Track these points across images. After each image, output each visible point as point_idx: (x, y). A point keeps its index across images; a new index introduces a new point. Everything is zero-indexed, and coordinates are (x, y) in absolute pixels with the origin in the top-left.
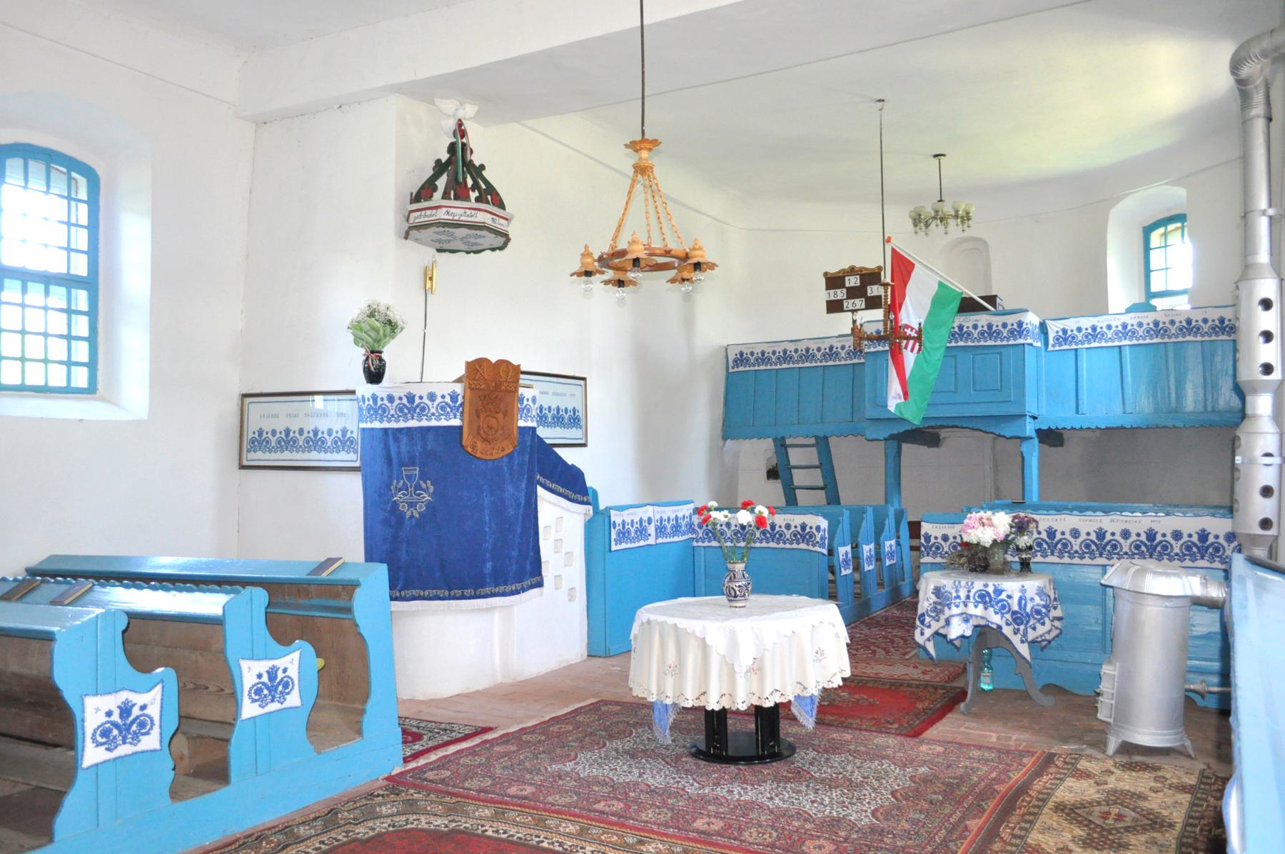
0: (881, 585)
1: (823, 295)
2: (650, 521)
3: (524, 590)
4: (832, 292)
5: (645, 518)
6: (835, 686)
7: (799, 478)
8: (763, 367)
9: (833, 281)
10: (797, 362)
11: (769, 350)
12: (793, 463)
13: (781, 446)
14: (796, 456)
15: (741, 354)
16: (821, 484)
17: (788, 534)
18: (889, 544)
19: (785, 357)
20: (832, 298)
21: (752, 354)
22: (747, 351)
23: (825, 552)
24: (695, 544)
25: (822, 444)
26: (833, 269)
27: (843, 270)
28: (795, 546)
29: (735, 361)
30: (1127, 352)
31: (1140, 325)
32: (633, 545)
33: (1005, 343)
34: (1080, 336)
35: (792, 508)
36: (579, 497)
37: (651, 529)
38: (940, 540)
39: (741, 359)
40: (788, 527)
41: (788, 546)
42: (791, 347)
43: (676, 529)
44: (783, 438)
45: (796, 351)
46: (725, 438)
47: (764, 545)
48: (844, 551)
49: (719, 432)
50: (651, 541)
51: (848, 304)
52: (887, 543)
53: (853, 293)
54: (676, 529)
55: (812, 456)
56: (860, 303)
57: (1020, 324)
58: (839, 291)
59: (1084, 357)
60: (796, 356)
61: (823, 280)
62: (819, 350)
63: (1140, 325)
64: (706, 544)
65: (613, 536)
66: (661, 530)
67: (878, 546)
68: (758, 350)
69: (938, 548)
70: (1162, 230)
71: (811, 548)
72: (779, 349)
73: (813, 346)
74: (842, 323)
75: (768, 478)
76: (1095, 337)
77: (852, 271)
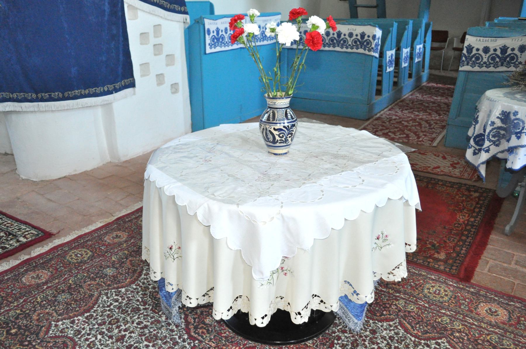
0: (410, 76)
3: (117, 90)
6: (398, 279)
16: (375, 4)
17: (350, 41)
18: (419, 47)
23: (377, 55)
28: (355, 50)
32: (227, 48)
35: (355, 20)
36: (177, 7)
38: (481, 52)
41: (349, 50)
47: (331, 48)
48: (390, 54)
52: (418, 47)
65: (208, 41)
67: (412, 48)
69: (477, 59)
71: (367, 52)
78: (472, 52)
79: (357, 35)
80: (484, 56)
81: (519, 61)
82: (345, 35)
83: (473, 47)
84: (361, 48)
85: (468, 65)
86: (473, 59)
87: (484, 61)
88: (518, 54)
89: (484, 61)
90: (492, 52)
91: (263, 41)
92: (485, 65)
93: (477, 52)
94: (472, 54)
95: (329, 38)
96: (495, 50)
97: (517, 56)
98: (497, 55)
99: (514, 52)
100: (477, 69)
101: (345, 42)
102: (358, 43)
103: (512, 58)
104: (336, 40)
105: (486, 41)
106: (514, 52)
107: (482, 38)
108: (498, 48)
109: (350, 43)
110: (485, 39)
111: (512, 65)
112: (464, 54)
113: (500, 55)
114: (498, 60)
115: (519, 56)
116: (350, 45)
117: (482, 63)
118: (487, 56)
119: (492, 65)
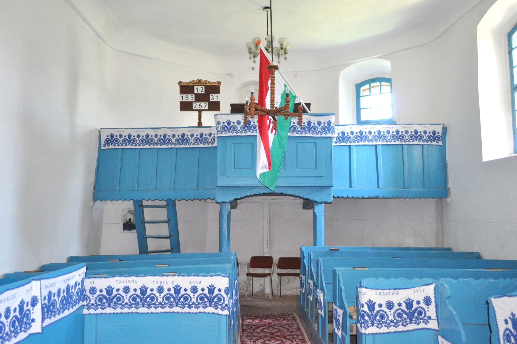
1: (179, 98)
2: (34, 302)
4: (184, 96)
5: (28, 299)
7: (150, 230)
8: (129, 147)
9: (186, 89)
10: (157, 144)
11: (134, 134)
12: (146, 219)
13: (139, 206)
14: (148, 214)
15: (112, 136)
16: (167, 234)
19: (147, 140)
20: (184, 100)
21: (121, 136)
22: (116, 134)
24: (85, 311)
25: (171, 205)
26: (186, 80)
27: (193, 82)
28: (201, 310)
29: (107, 141)
30: (380, 149)
31: (388, 132)
33: (319, 135)
34: (352, 137)
37: (37, 313)
38: (384, 308)
39: (112, 140)
40: (194, 289)
42: (152, 133)
43: (67, 302)
44: (141, 201)
45: (156, 136)
46: (95, 199)
47: (167, 309)
49: (90, 195)
50: (36, 328)
51: (196, 105)
53: (199, 98)
54: (67, 302)
55: (162, 214)
56: (204, 105)
57: (329, 123)
58: (189, 95)
59: (354, 150)
60: (156, 140)
61: (178, 87)
62: (174, 136)
63: (388, 132)
64: (99, 311)
66: (48, 310)
68: (126, 133)
69: (382, 317)
70: (367, 86)
72: (143, 134)
73: (169, 133)
74: (190, 118)
75: (124, 229)
76: (361, 138)
77: (199, 83)
78: (374, 309)
79: (203, 290)
80: (389, 313)
81: (427, 315)
82: (186, 290)
83: (375, 303)
84: (210, 306)
85: (373, 325)
86: (378, 318)
87: (390, 319)
88: (425, 307)
89: (390, 319)
90: (396, 307)
91: (63, 312)
92: (392, 324)
93: (380, 309)
94: (375, 312)
95: (163, 295)
96: (400, 305)
97: (424, 310)
98: (402, 310)
99: (420, 305)
100: (384, 330)
101: (186, 299)
102: (206, 300)
103: (420, 313)
104: (174, 298)
105: (387, 294)
106: (420, 305)
107: (381, 291)
108: (402, 302)
109: (194, 300)
110: (385, 291)
111: (422, 321)
112: (365, 312)
113: (406, 310)
114: (405, 316)
115: (426, 310)
116: (194, 303)
117: (389, 322)
118: (392, 313)
119: (401, 323)
